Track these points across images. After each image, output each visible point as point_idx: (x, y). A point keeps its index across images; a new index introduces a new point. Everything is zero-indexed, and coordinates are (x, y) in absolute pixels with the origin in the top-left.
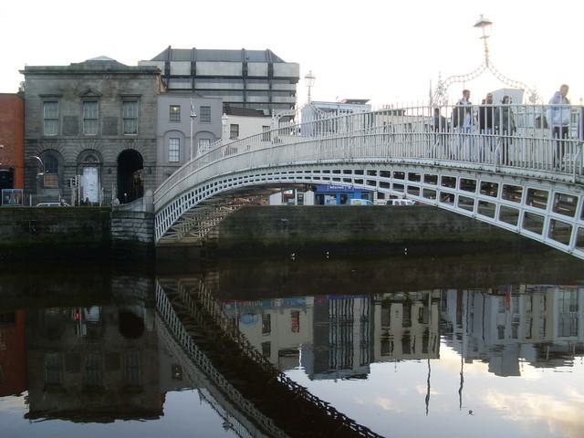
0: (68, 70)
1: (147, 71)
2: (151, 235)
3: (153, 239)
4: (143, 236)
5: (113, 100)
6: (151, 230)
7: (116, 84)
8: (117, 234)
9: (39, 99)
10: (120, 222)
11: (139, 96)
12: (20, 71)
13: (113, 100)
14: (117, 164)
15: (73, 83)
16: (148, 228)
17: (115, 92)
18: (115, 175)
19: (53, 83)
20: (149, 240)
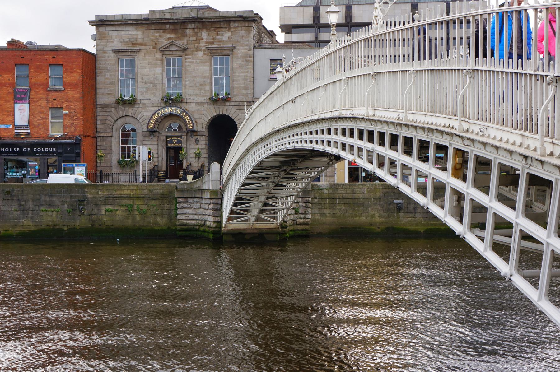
0: (145, 19)
1: (240, 17)
3: (220, 223)
4: (211, 221)
5: (201, 54)
6: (218, 211)
7: (204, 34)
8: (183, 217)
9: (113, 55)
10: (187, 202)
11: (233, 49)
12: (90, 22)
13: (201, 54)
14: (207, 133)
15: (154, 34)
16: (214, 209)
17: (202, 44)
18: (204, 147)
19: (130, 33)
20: (215, 225)
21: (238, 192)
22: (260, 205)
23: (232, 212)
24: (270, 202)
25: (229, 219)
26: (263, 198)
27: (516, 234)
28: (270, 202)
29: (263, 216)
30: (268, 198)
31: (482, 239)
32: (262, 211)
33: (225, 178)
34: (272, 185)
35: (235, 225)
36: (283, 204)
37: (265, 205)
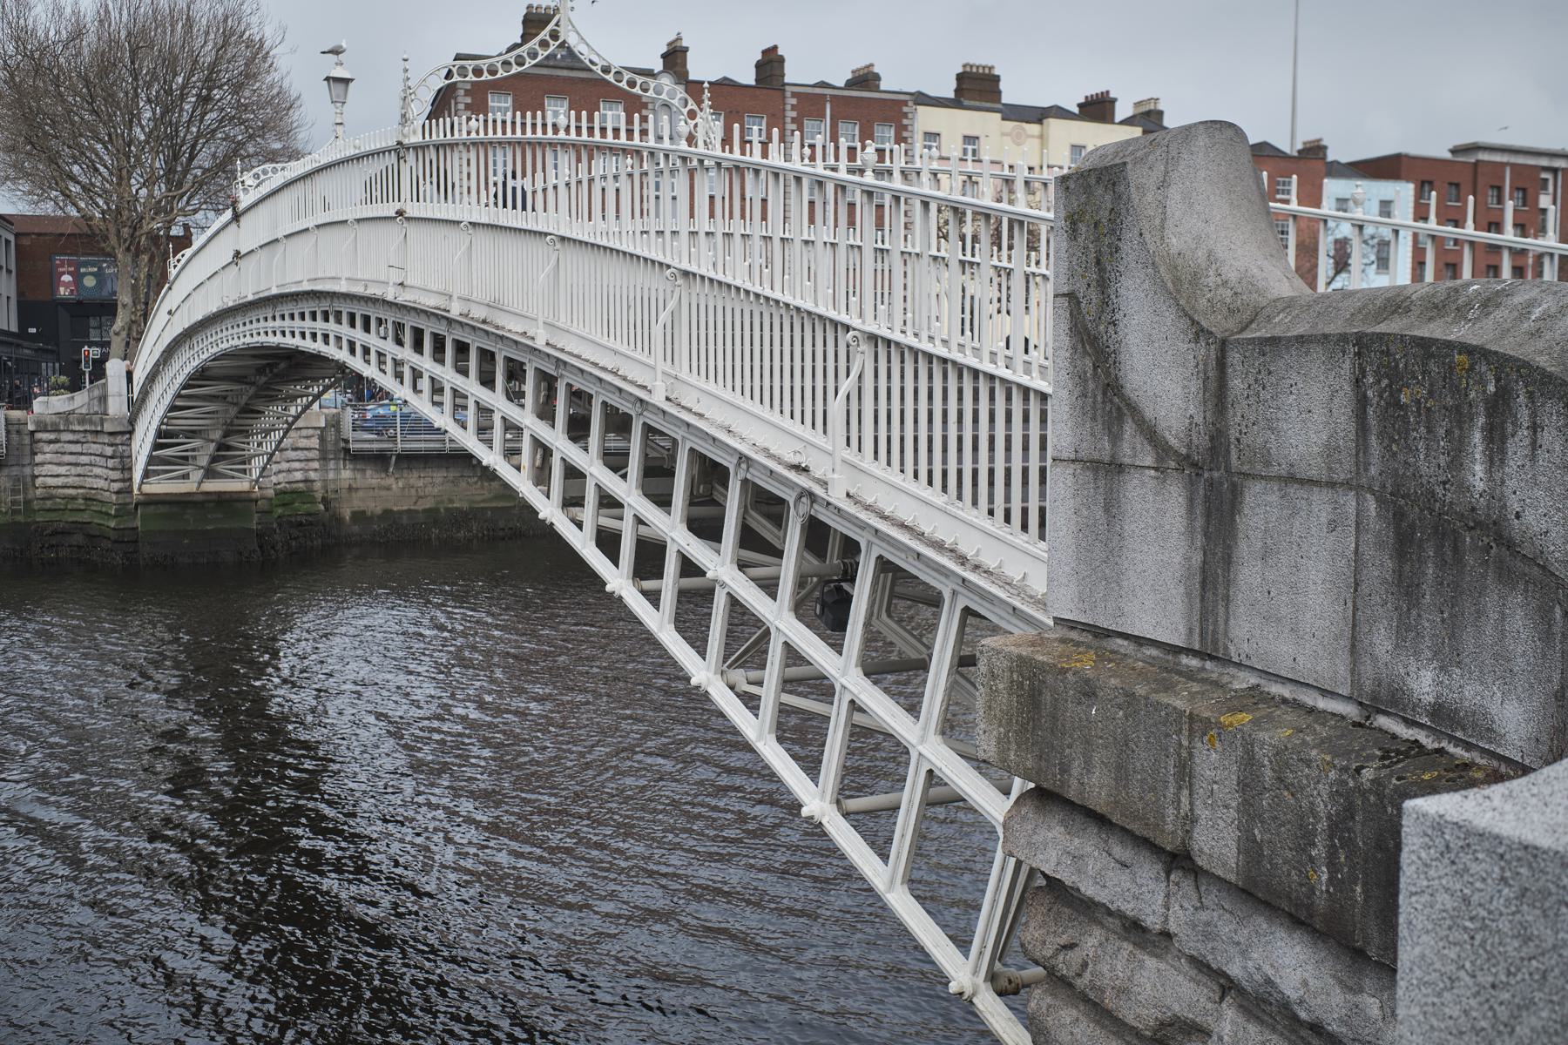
2: (127, 476)
21: (162, 423)
22: (212, 446)
23: (151, 460)
24: (233, 441)
25: (147, 474)
26: (217, 435)
27: (628, 515)
28: (233, 441)
29: (220, 467)
30: (226, 435)
31: (579, 525)
32: (214, 459)
33: (136, 390)
34: (233, 411)
35: (158, 486)
36: (260, 444)
37: (222, 447)
